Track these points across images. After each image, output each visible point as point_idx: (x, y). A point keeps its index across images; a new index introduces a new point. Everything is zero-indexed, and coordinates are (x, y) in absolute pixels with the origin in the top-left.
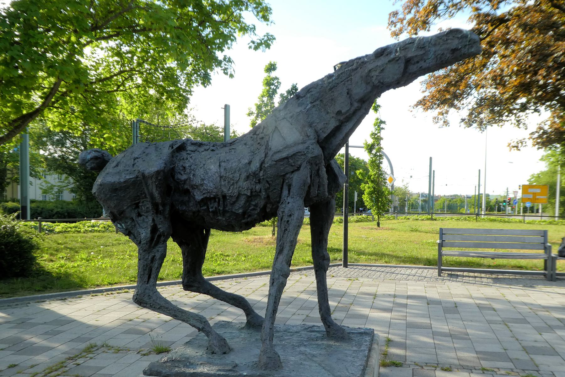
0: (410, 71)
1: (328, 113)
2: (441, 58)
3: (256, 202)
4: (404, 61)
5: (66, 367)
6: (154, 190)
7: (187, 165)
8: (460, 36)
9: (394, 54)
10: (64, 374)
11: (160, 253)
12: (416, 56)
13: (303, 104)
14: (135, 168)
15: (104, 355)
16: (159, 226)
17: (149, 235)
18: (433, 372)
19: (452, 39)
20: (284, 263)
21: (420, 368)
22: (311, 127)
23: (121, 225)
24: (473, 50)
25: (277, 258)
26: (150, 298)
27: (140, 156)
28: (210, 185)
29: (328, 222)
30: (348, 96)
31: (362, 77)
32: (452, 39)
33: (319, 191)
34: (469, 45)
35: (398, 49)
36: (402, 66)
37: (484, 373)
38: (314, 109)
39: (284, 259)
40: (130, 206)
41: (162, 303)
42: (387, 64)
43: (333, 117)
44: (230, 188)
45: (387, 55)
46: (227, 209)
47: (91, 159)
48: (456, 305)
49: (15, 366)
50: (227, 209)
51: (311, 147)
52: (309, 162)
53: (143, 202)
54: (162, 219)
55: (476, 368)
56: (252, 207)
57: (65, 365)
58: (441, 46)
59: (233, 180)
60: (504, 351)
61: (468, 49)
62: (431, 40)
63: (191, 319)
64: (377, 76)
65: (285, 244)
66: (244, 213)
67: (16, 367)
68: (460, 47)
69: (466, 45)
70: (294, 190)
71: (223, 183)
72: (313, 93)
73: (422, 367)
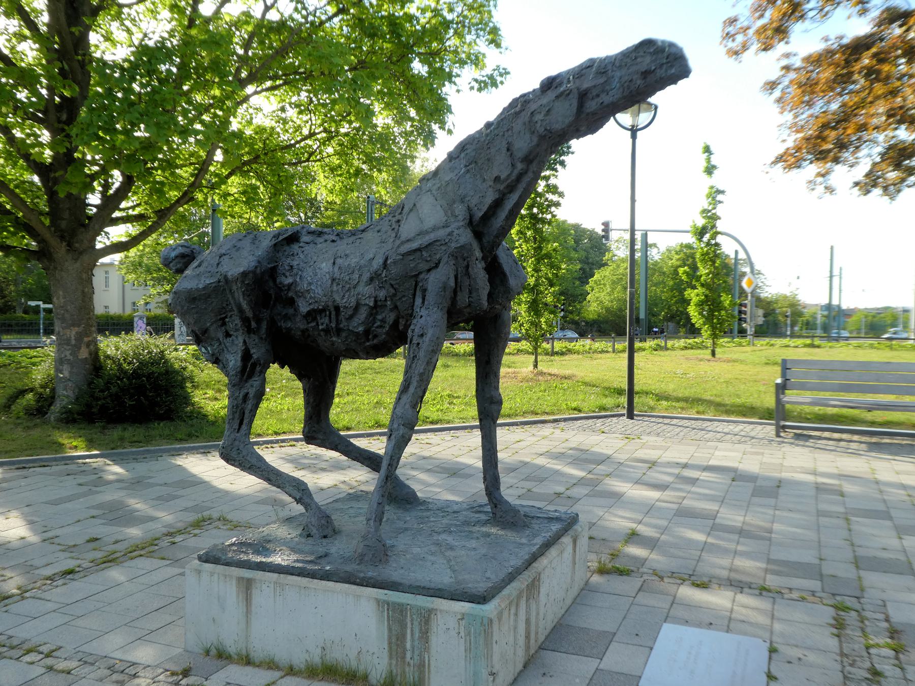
0: (588, 111)
1: (484, 180)
2: (629, 87)
3: (384, 315)
4: (576, 96)
5: (156, 545)
6: (241, 300)
7: (295, 263)
8: (652, 50)
9: (565, 86)
10: (148, 555)
11: (254, 389)
12: (595, 86)
13: (456, 168)
14: (220, 269)
15: (215, 531)
16: (252, 351)
17: (239, 364)
18: (675, 587)
19: (642, 56)
20: (408, 406)
21: (657, 578)
22: (463, 202)
23: (206, 349)
24: (673, 71)
25: (400, 399)
26: (239, 453)
27: (228, 252)
28: (318, 292)
29: (498, 346)
30: (509, 153)
31: (525, 124)
32: (642, 56)
33: (470, 299)
34: (668, 63)
35: (571, 77)
36: (575, 103)
37: (761, 594)
38: (468, 176)
39: (409, 400)
40: (215, 322)
41: (254, 461)
42: (554, 101)
43: (490, 186)
44: (344, 296)
45: (556, 87)
46: (342, 326)
47: (176, 257)
48: (780, 484)
49: (97, 539)
50: (342, 326)
51: (456, 232)
52: (453, 256)
53: (231, 316)
54: (257, 341)
55: (753, 586)
56: (378, 323)
57: (156, 542)
58: (628, 69)
59: (350, 284)
60: (817, 561)
61: (666, 71)
62: (615, 59)
63: (287, 485)
64: (541, 120)
65: (413, 378)
66: (367, 332)
67: (97, 542)
68: (653, 68)
69: (663, 64)
70: (430, 297)
71: (335, 288)
72: (468, 151)
73: (662, 578)
